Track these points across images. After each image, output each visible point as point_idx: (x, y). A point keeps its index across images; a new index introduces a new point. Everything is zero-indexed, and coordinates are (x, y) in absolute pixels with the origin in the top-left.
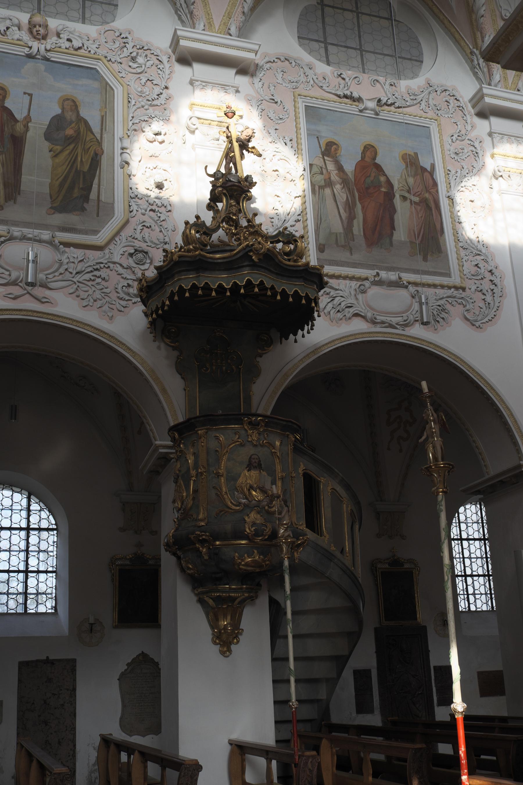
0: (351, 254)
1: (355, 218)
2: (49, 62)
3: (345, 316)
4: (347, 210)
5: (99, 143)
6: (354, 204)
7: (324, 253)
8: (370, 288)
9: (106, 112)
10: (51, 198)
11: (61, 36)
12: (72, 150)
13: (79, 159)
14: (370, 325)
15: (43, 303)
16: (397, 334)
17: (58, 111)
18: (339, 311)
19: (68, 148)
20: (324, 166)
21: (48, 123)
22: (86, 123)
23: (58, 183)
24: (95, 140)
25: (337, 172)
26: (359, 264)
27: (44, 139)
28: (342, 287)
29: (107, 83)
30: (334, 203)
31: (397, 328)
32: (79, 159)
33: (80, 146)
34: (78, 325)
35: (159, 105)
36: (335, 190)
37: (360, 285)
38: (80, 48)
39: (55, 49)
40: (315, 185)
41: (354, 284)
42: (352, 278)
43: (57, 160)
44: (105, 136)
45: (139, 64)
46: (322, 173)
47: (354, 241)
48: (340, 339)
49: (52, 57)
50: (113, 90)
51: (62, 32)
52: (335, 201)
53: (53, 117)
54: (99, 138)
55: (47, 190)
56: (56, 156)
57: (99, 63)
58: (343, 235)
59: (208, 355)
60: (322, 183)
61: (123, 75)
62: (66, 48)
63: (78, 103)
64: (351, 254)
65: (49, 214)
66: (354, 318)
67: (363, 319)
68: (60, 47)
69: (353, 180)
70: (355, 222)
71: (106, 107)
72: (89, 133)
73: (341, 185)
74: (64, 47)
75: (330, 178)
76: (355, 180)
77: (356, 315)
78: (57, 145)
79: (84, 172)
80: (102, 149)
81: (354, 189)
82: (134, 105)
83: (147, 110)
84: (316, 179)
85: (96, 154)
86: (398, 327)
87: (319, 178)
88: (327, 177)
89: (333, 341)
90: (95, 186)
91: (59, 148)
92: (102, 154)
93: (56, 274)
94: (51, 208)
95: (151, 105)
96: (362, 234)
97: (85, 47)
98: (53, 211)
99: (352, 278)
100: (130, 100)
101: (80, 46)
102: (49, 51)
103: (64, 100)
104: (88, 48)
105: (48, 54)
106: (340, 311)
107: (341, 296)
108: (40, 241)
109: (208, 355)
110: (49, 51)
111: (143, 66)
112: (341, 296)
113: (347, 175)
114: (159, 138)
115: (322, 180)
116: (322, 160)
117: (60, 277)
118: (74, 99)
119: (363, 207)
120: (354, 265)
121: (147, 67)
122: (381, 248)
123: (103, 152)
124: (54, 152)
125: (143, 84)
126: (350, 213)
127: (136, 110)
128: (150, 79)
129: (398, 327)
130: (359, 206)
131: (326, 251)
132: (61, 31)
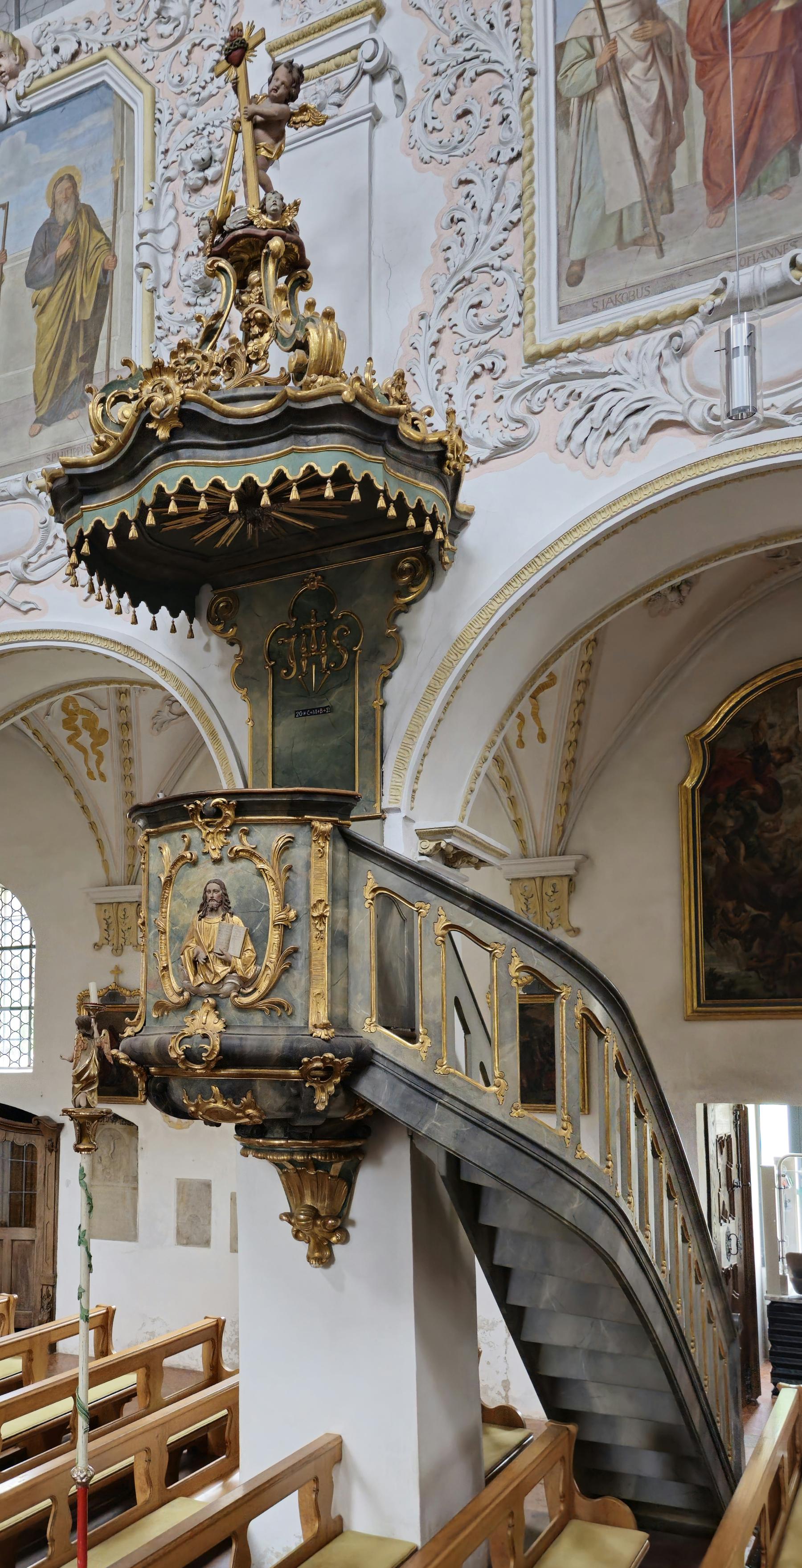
0: (661, 252)
1: (680, 138)
2: (32, 119)
3: (628, 439)
4: (659, 127)
5: (110, 244)
6: (682, 96)
7: (582, 284)
8: (701, 333)
9: (122, 168)
10: (36, 399)
11: (43, 49)
12: (67, 286)
13: (78, 297)
14: (706, 440)
15: (26, 612)
16: (786, 442)
17: (45, 213)
18: (608, 434)
19: (59, 285)
20: (599, 31)
21: (30, 249)
22: (89, 211)
23: (45, 366)
24: (103, 242)
25: (636, 26)
26: (682, 273)
27: (25, 285)
28: (619, 363)
29: (124, 102)
30: (621, 125)
31: (782, 425)
32: (78, 297)
33: (79, 270)
34: (77, 638)
35: (214, 93)
36: (626, 86)
37: (672, 337)
38: (75, 55)
39: (33, 86)
40: (568, 100)
41: (657, 339)
42: (651, 326)
43: (44, 319)
44: (120, 223)
45: (176, 19)
46: (591, 55)
47: (671, 210)
48: (609, 506)
49: (31, 107)
50: (132, 110)
51: (42, 41)
52: (626, 116)
53: (38, 232)
54: (109, 235)
55: (29, 389)
56: (42, 312)
57: (106, 68)
58: (638, 210)
59: (293, 640)
60: (592, 82)
61: (149, 64)
62: (53, 70)
63: (76, 178)
64: (661, 252)
65: (34, 436)
66: (655, 436)
67: (684, 430)
68: (40, 77)
69: (683, 26)
70: (681, 152)
71: (122, 158)
72: (95, 232)
73: (644, 60)
74: (47, 70)
75: (613, 58)
76: (689, 25)
77: (660, 426)
78: (43, 288)
79: (85, 321)
80: (114, 256)
81: (683, 53)
82: (170, 121)
83: (191, 119)
84: (573, 81)
85: (105, 272)
86: (788, 418)
87: (584, 75)
88: (606, 57)
89: (588, 519)
90: (102, 342)
91: (46, 291)
92: (115, 267)
93: (43, 551)
94: (37, 421)
95: (200, 103)
96: (700, 176)
97: (84, 47)
98: (38, 426)
99: (651, 326)
100: (158, 115)
101: (73, 51)
102: (25, 95)
103: (55, 186)
104: (87, 45)
105: (25, 103)
106: (612, 431)
107: (614, 390)
108: (11, 498)
109: (293, 640)
110: (25, 95)
111: (183, 19)
112: (614, 390)
113: (666, 19)
114: (210, 173)
115: (589, 75)
116: (594, 15)
117: (50, 555)
118: (71, 173)
119: (708, 95)
120: (669, 283)
121: (192, 15)
122: (759, 193)
123: (116, 261)
124: (40, 305)
125: (185, 61)
126: (668, 130)
127: (173, 131)
128: (197, 41)
129: (788, 418)
130: (696, 94)
131: (588, 275)
132: (38, 40)
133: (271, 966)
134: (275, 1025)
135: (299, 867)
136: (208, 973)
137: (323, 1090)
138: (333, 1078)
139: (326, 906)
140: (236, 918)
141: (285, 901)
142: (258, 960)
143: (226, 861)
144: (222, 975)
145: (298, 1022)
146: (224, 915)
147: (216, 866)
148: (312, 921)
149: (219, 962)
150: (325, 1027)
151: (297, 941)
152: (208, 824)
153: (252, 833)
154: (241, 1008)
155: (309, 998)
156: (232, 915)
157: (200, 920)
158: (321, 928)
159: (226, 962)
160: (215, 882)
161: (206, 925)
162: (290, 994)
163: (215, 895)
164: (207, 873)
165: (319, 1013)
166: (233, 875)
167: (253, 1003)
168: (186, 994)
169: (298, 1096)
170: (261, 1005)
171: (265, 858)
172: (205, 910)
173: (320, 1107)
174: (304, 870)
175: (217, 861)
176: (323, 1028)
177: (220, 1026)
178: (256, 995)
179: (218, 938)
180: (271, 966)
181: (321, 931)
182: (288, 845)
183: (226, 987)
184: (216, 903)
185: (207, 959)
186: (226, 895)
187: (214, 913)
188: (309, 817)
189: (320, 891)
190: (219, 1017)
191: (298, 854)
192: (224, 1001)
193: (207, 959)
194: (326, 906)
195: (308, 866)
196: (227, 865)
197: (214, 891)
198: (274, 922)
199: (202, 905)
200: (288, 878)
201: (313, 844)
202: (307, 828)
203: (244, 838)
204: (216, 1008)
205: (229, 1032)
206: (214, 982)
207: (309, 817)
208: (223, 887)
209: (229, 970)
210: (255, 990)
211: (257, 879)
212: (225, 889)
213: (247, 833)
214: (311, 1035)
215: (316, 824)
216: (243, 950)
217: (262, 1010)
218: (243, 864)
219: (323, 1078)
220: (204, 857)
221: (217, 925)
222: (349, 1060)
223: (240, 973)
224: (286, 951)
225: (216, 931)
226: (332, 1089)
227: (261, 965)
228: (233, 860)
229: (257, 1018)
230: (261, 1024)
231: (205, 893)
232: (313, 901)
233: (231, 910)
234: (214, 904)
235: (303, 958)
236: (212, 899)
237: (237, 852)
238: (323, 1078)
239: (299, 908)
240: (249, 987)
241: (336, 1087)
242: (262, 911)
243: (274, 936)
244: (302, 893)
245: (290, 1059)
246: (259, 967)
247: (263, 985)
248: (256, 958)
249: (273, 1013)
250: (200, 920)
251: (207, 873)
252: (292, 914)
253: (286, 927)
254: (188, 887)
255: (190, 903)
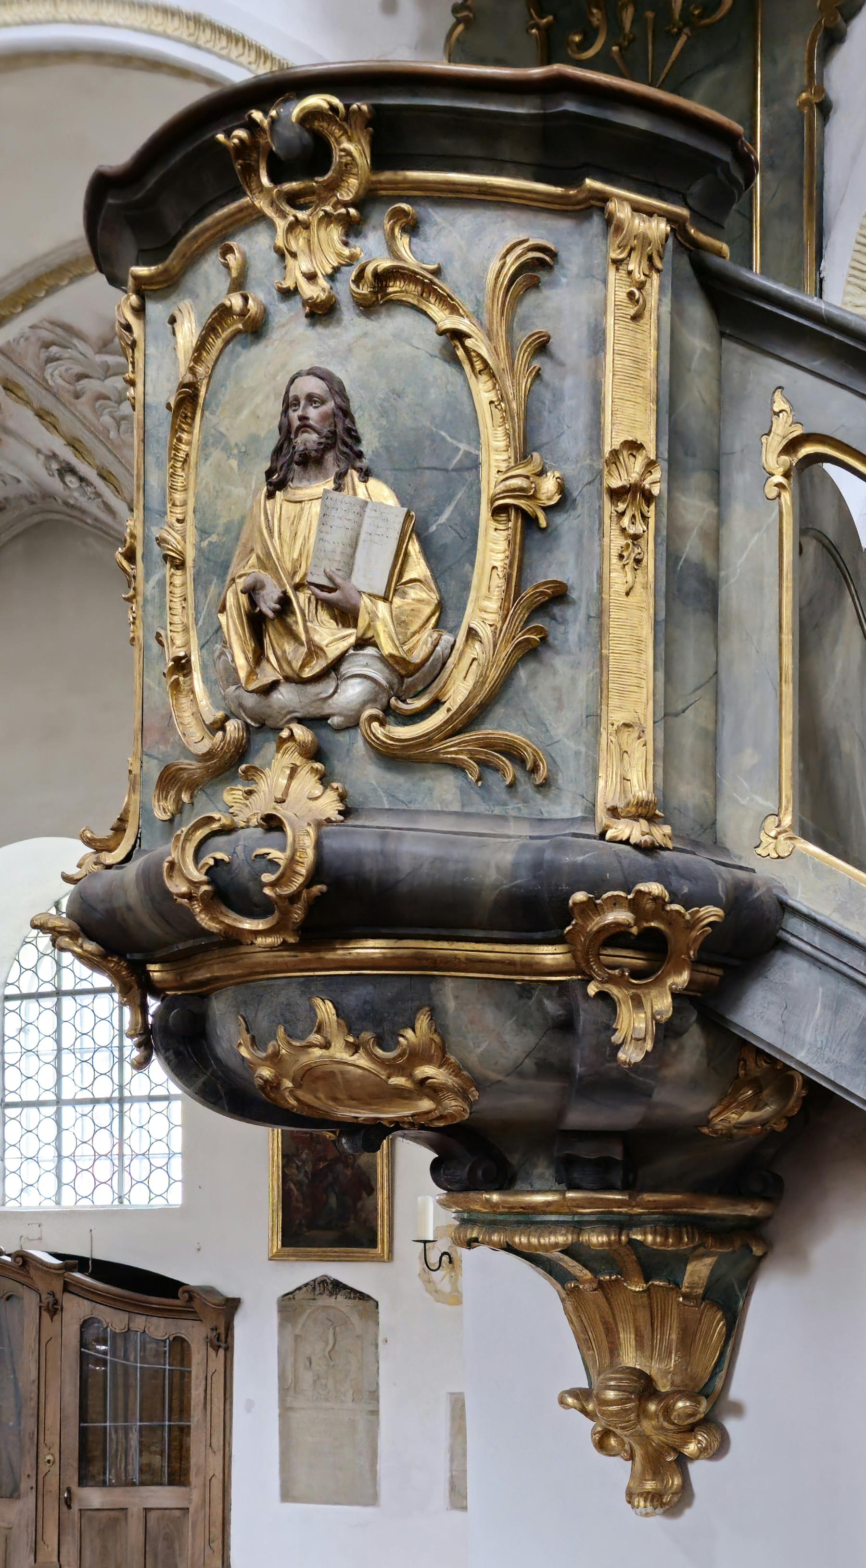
133: (485, 632)
134: (497, 811)
135: (569, 343)
136: (289, 647)
137: (638, 1003)
138: (668, 974)
139: (650, 465)
140: (379, 492)
141: (525, 447)
142: (445, 614)
143: (348, 312)
144: (333, 652)
145: (564, 807)
146: (340, 477)
147: (319, 329)
148: (608, 508)
149: (324, 616)
150: (645, 812)
151: (559, 566)
152: (294, 200)
153: (427, 230)
154: (394, 758)
155: (597, 733)
156: (366, 475)
157: (270, 495)
158: (639, 528)
159: (345, 615)
160: (312, 372)
161: (290, 509)
162: (541, 722)
163: (313, 414)
164: (295, 348)
165: (629, 773)
166: (377, 360)
167: (427, 739)
168: (232, 726)
169: (565, 1022)
170: (451, 748)
171: (467, 307)
172: (286, 466)
173: (631, 1055)
174: (585, 351)
175: (322, 313)
176: (636, 817)
177: (328, 805)
178: (438, 718)
179: (320, 539)
180: (485, 632)
181: (636, 537)
182: (536, 269)
183: (351, 693)
184: (318, 443)
185: (285, 602)
186: (345, 412)
187: (312, 471)
188: (597, 185)
189: (632, 416)
190: (325, 779)
191: (561, 306)
192: (343, 738)
193: (285, 602)
194: (650, 465)
195: (597, 340)
196: (352, 325)
197: (311, 399)
198: (493, 500)
199: (277, 452)
200: (538, 375)
201: (612, 274)
202: (596, 223)
203: (403, 243)
204: (316, 754)
205: (350, 822)
206: (307, 673)
207: (597, 185)
208: (337, 389)
209: (352, 640)
210: (436, 704)
211: (441, 369)
212: (346, 399)
213: (412, 228)
214: (602, 836)
215: (622, 212)
216: (396, 583)
217: (456, 767)
218: (398, 322)
219: (637, 973)
220: (283, 307)
221: (316, 508)
222: (711, 913)
223: (388, 648)
224: (528, 592)
225: (315, 523)
226: (662, 1004)
227: (454, 631)
228: (367, 308)
229: (445, 789)
230: (456, 807)
231: (285, 412)
232: (612, 441)
233: (365, 463)
234: (309, 440)
235: (582, 615)
236: (305, 425)
237: (382, 278)
238: (637, 973)
239: (569, 470)
240: (417, 695)
241: (675, 996)
242: (459, 469)
243: (494, 545)
244: (580, 424)
245: (535, 909)
246: (447, 638)
247: (459, 690)
248: (440, 606)
249: (492, 778)
250: (270, 495)
251: (295, 348)
252: (548, 486)
253: (529, 521)
254: (239, 410)
255: (244, 456)
